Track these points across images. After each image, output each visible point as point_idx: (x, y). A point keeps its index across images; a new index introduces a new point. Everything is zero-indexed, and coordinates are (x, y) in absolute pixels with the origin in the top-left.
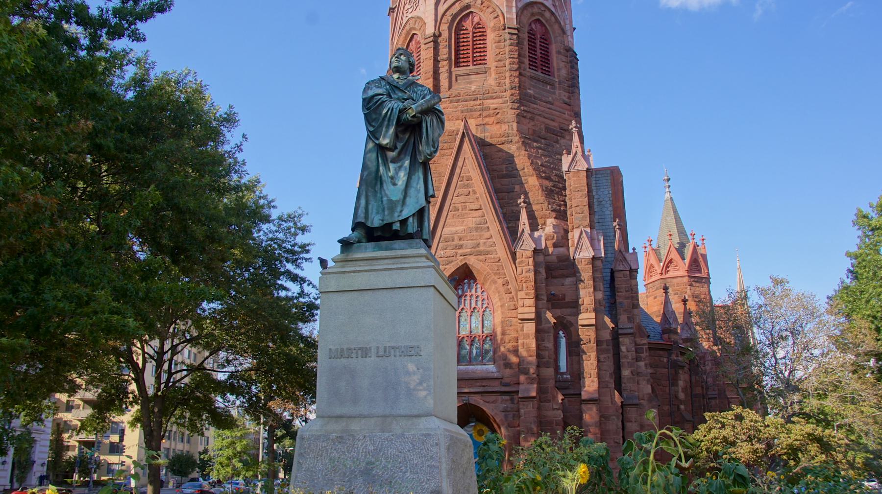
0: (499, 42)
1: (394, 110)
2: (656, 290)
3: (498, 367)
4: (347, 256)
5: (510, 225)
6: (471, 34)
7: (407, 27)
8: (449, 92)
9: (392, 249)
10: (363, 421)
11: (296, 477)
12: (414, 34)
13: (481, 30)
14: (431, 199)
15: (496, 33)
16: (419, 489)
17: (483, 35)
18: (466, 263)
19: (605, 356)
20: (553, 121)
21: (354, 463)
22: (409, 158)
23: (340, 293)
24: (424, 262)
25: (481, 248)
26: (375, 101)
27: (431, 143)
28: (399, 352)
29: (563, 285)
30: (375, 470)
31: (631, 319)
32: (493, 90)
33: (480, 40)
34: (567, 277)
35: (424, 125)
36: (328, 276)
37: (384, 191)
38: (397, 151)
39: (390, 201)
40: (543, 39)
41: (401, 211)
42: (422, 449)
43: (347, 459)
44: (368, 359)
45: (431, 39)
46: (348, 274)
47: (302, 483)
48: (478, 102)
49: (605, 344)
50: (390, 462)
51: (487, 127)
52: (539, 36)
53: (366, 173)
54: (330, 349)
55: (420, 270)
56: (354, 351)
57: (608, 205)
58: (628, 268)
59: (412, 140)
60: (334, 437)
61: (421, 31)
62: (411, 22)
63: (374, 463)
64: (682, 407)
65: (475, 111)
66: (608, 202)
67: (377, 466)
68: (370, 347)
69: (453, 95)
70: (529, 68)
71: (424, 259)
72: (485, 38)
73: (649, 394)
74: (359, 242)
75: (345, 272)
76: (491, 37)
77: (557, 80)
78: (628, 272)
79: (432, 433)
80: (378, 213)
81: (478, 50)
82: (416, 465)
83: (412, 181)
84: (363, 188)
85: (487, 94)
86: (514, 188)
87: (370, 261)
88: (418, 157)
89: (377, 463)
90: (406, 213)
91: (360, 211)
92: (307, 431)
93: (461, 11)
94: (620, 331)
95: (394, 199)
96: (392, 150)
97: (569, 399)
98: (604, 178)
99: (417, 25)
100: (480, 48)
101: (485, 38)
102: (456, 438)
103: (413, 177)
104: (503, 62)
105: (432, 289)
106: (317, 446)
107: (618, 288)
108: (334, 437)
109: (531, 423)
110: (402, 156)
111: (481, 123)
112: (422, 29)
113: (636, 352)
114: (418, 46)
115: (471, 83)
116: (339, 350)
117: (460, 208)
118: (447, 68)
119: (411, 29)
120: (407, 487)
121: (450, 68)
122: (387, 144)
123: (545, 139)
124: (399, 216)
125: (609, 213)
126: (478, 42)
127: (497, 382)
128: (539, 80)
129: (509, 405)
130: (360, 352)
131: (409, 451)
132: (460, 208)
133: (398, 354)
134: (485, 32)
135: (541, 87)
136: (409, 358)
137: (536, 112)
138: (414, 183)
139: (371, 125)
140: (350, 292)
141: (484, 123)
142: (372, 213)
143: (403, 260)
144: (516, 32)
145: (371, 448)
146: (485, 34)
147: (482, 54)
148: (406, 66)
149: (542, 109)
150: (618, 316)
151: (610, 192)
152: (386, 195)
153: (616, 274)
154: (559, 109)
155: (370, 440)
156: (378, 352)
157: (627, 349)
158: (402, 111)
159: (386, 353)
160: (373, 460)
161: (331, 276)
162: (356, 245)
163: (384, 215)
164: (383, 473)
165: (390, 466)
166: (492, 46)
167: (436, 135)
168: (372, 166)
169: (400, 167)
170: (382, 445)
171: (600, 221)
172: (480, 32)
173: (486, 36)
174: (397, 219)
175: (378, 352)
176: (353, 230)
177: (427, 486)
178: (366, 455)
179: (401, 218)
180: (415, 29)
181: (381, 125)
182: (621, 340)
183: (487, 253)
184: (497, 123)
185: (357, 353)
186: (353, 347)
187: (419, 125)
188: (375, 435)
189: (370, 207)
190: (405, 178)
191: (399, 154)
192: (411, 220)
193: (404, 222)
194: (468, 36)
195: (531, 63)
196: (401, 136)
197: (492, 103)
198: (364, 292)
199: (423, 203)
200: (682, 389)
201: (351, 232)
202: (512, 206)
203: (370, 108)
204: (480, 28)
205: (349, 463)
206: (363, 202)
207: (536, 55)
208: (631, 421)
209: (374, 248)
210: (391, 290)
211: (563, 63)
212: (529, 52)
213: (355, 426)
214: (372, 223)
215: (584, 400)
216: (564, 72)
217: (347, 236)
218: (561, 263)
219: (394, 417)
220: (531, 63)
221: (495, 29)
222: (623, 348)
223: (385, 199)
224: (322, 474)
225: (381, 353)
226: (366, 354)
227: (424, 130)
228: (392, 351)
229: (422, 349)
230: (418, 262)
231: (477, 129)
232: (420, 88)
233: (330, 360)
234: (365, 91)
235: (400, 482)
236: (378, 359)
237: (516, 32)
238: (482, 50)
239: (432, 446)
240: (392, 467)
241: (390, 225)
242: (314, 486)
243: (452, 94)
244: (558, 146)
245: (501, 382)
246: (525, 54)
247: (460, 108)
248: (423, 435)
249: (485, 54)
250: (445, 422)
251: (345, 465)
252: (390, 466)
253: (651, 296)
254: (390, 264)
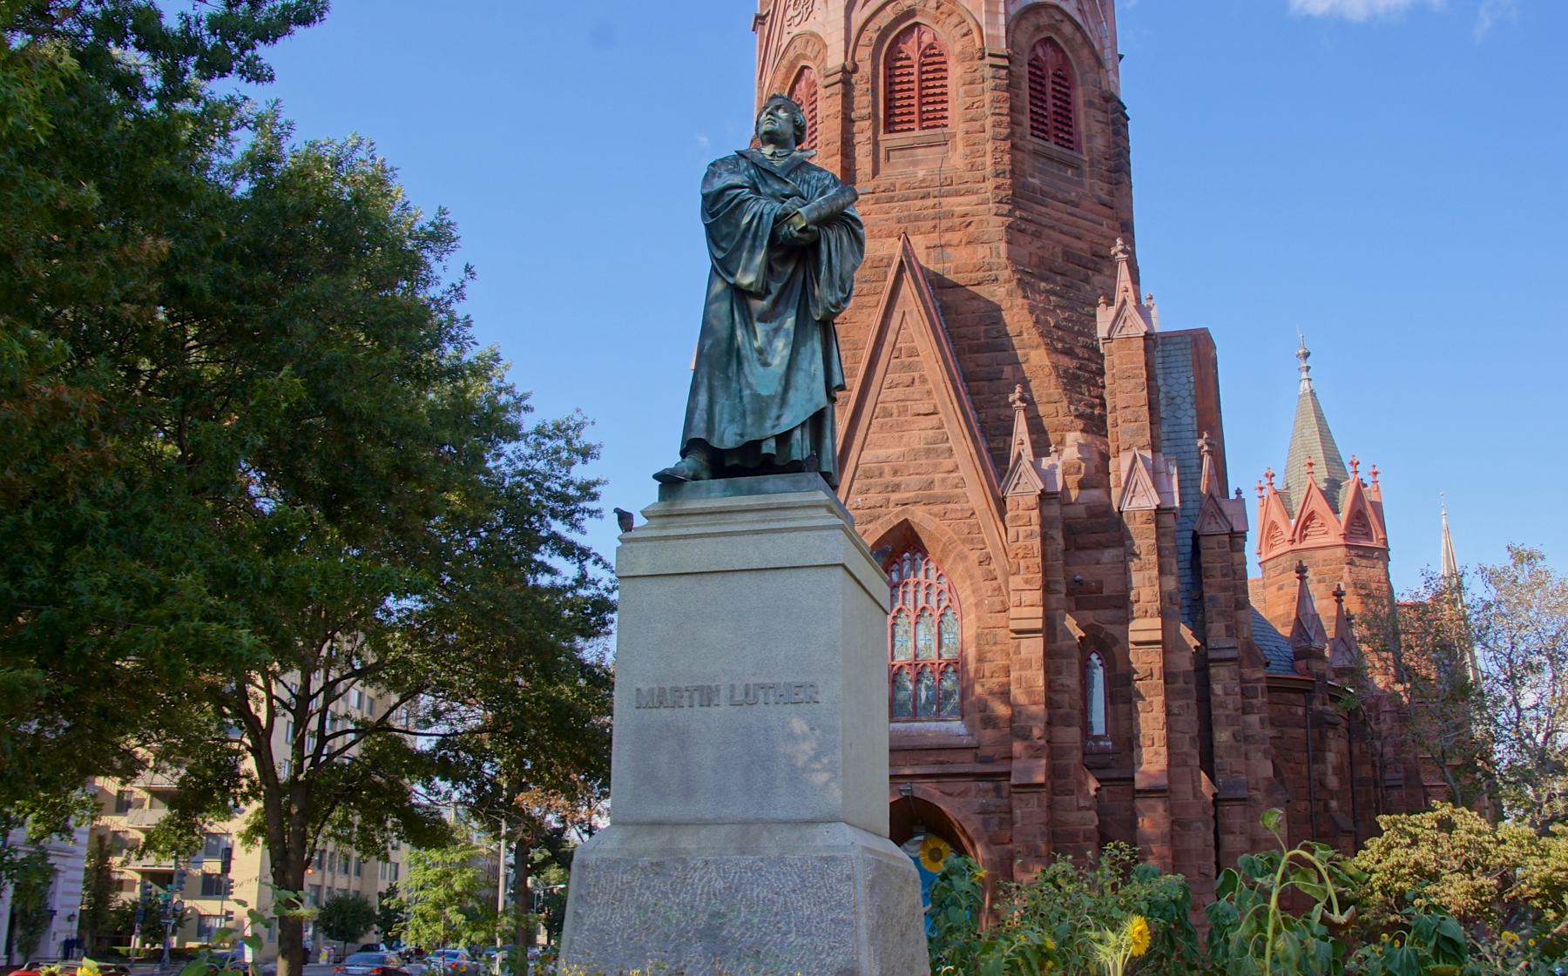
0: (971, 83)
1: (765, 217)
3: (971, 726)
4: (672, 505)
5: (994, 445)
6: (916, 66)
7: (791, 54)
8: (874, 183)
9: (760, 492)
10: (704, 831)
11: (572, 942)
12: (804, 68)
13: (936, 59)
14: (838, 394)
15: (967, 64)
16: (813, 966)
17: (941, 70)
18: (906, 520)
20: (1079, 238)
21: (685, 914)
22: (794, 312)
23: (659, 580)
24: (825, 517)
25: (937, 490)
26: (727, 199)
27: (837, 283)
28: (775, 695)
29: (1098, 563)
30: (727, 928)
31: (1232, 631)
32: (960, 177)
33: (934, 79)
34: (1107, 547)
35: (824, 247)
36: (634, 545)
37: (746, 377)
38: (770, 298)
39: (757, 397)
40: (1059, 76)
41: (779, 417)
42: (820, 888)
43: (671, 907)
44: (713, 710)
45: (838, 77)
46: (673, 542)
47: (583, 953)
48: (930, 202)
49: (1181, 680)
50: (756, 912)
51: (949, 250)
52: (1050, 72)
53: (708, 342)
54: (638, 690)
55: (817, 533)
56: (686, 694)
57: (1188, 406)
58: (1227, 530)
59: (801, 277)
60: (647, 864)
61: (818, 62)
62: (798, 42)
63: (724, 915)
64: (1334, 804)
65: (925, 219)
66: (1189, 399)
67: (730, 920)
68: (717, 686)
69: (882, 189)
70: (1032, 134)
71: (823, 512)
72: (944, 74)
73: (1268, 779)
74: (695, 478)
75: (666, 538)
76: (956, 73)
77: (1086, 158)
78: (1226, 538)
79: (840, 855)
80: (732, 421)
81: (931, 99)
82: (809, 919)
83: (800, 357)
84: (704, 370)
85: (948, 186)
86: (1002, 372)
87: (718, 516)
88: (812, 310)
89: (731, 916)
90: (787, 423)
91: (697, 416)
92: (592, 851)
93: (898, 20)
94: (1211, 655)
95: (764, 392)
96: (760, 296)
97: (1111, 788)
98: (1179, 352)
99: (809, 49)
100: (934, 94)
101: (944, 74)
102: (888, 866)
103: (802, 350)
104: (979, 123)
105: (840, 571)
106: (612, 881)
107: (1206, 568)
108: (647, 864)
109: (1035, 836)
110: (781, 308)
111: (937, 242)
112: (820, 57)
113: (1244, 694)
114: (812, 91)
115: (915, 163)
116: (656, 693)
117: (895, 412)
118: (869, 133)
119: (798, 58)
120: (790, 962)
121: (876, 133)
122: (751, 284)
123: (1062, 274)
124: (774, 427)
125: (1189, 420)
126: (931, 84)
127: (969, 756)
128: (1050, 159)
129: (992, 799)
130: (696, 696)
131: (794, 891)
132: (895, 412)
133: (772, 699)
134: (945, 62)
135: (1055, 171)
136: (793, 706)
137: (1044, 221)
138: (803, 362)
139: (719, 248)
140: (677, 578)
141: (943, 242)
142: (721, 422)
143: (783, 514)
144: (1005, 63)
145: (719, 885)
146: (944, 66)
147: (939, 107)
148: (789, 129)
149: (1058, 215)
150: (1208, 625)
151: (1192, 379)
152: (750, 386)
153: (1203, 542)
154: (1090, 216)
155: (718, 869)
156: (732, 696)
157: (1225, 688)
158: (780, 220)
159: (748, 697)
160: (723, 909)
161: (642, 544)
162: (690, 484)
163: (745, 424)
164: (743, 935)
165: (756, 920)
166: (957, 91)
167: (848, 266)
168: (722, 328)
169: (776, 331)
170: (741, 878)
171: (1172, 436)
172: (934, 63)
173: (946, 70)
174: (770, 433)
175: (732, 696)
176: (684, 454)
177: (829, 960)
178: (710, 899)
179: (778, 431)
180: (805, 57)
181: (738, 248)
182: (1212, 671)
183: (948, 500)
184: (969, 243)
185: (691, 697)
186: (682, 685)
187: (815, 246)
188: (728, 860)
189: (717, 409)
190: (787, 352)
191: (776, 303)
192: (798, 434)
193: (784, 439)
194: (911, 70)
195: (1035, 125)
196: (777, 268)
197: (958, 204)
198: (707, 577)
199: (821, 399)
200: (1334, 768)
201: (680, 459)
202: (998, 407)
203: (718, 212)
204: (934, 55)
205: (675, 915)
206: (703, 399)
207: (1045, 109)
208: (1233, 833)
209: (725, 491)
210: (759, 573)
211: (1099, 125)
212: (1031, 103)
213: (687, 841)
214: (721, 440)
215: (1139, 791)
216: (1099, 143)
217: (672, 466)
218: (1094, 520)
219: (766, 823)
220: (1035, 125)
221: (964, 57)
222: (1217, 688)
223: (746, 392)
224: (622, 936)
225: (739, 697)
226: (710, 700)
227: (824, 257)
228: (761, 693)
229: (820, 689)
230: (811, 518)
231: (928, 255)
232: (816, 174)
233: (637, 711)
234: (707, 179)
235: (777, 952)
236: (733, 710)
237: (1005, 63)
238: (938, 99)
239: (839, 881)
240: (760, 922)
241: (756, 444)
242: (606, 961)
243: (878, 186)
244: (1088, 288)
245: (976, 755)
246: (1024, 108)
247: (894, 214)
248: (821, 859)
249: (944, 106)
250: (862, 832)
251: (667, 919)
252: (756, 920)
253: (1271, 585)
254: (757, 521)
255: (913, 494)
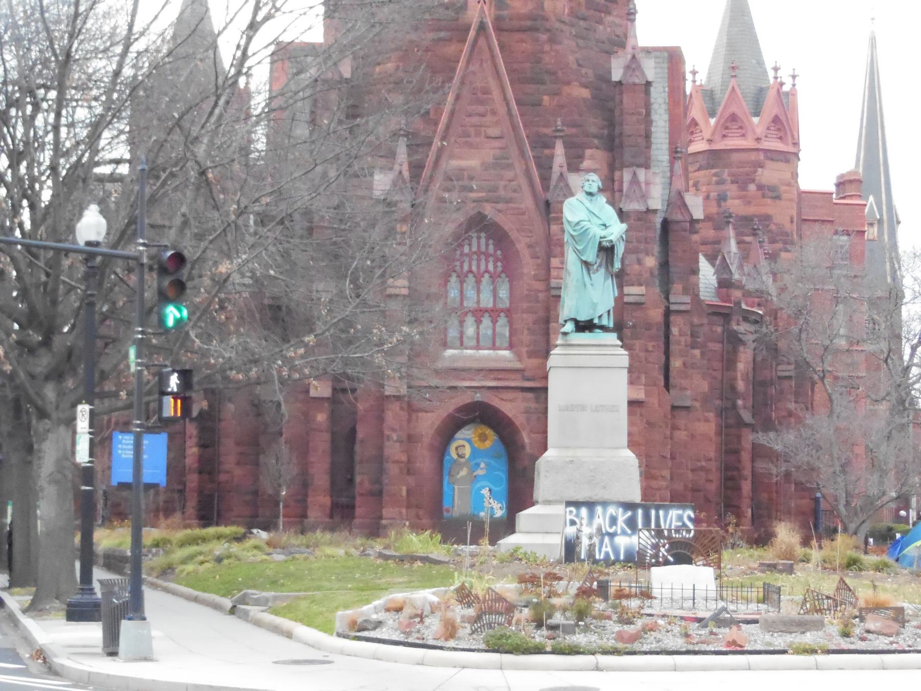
2: (698, 170)
18: (479, 213)
19: (653, 343)
25: (502, 193)
58: (688, 219)
64: (740, 402)
78: (688, 224)
86: (542, 100)
94: (673, 307)
113: (692, 335)
117: (472, 133)
127: (519, 376)
129: (533, 405)
132: (472, 133)
151: (667, 89)
157: (680, 330)
159: (598, 409)
200: (742, 375)
222: (675, 330)
244: (601, 27)
245: (523, 375)
255: (484, 194)
